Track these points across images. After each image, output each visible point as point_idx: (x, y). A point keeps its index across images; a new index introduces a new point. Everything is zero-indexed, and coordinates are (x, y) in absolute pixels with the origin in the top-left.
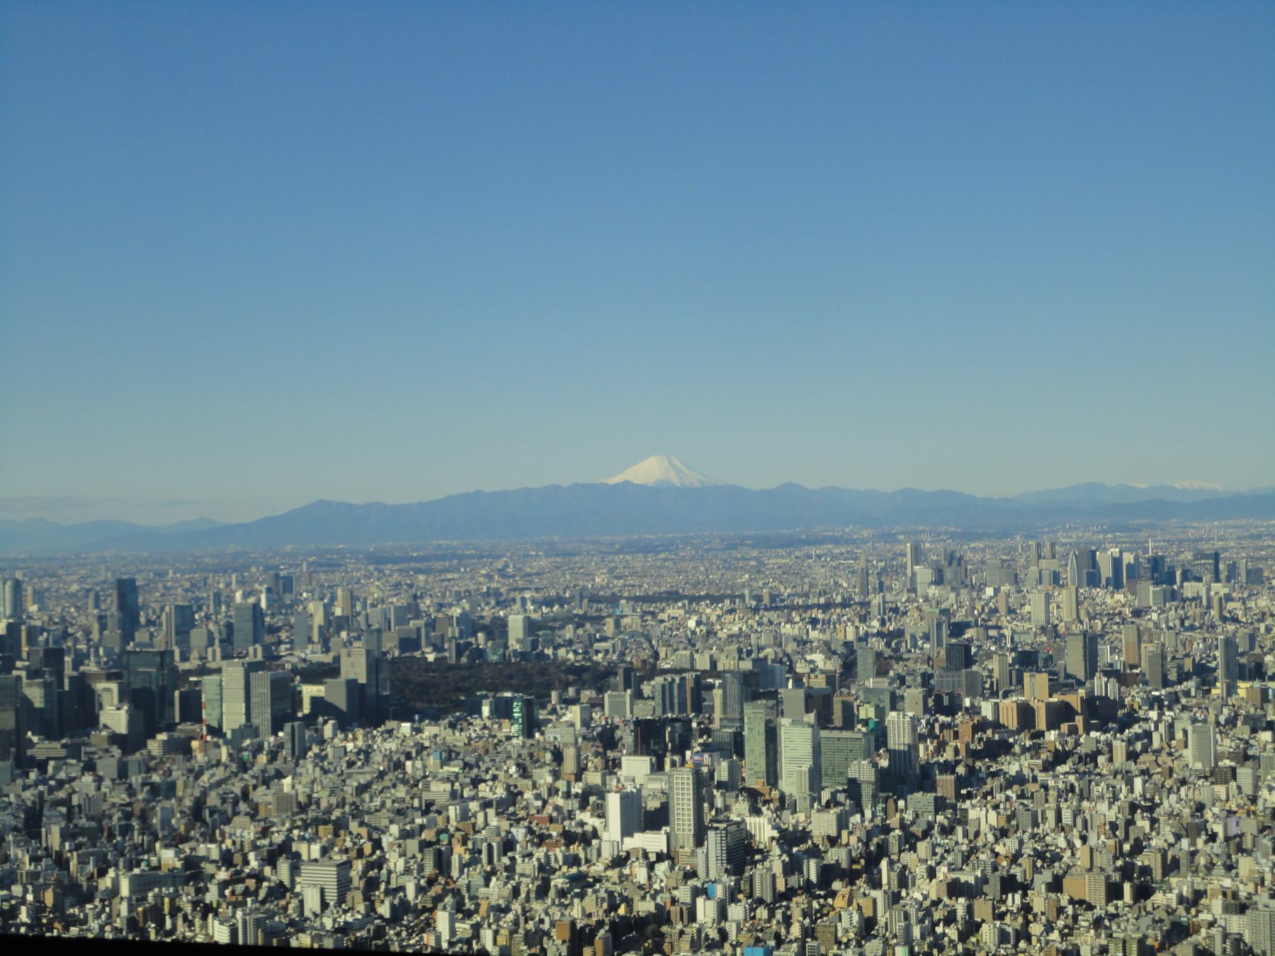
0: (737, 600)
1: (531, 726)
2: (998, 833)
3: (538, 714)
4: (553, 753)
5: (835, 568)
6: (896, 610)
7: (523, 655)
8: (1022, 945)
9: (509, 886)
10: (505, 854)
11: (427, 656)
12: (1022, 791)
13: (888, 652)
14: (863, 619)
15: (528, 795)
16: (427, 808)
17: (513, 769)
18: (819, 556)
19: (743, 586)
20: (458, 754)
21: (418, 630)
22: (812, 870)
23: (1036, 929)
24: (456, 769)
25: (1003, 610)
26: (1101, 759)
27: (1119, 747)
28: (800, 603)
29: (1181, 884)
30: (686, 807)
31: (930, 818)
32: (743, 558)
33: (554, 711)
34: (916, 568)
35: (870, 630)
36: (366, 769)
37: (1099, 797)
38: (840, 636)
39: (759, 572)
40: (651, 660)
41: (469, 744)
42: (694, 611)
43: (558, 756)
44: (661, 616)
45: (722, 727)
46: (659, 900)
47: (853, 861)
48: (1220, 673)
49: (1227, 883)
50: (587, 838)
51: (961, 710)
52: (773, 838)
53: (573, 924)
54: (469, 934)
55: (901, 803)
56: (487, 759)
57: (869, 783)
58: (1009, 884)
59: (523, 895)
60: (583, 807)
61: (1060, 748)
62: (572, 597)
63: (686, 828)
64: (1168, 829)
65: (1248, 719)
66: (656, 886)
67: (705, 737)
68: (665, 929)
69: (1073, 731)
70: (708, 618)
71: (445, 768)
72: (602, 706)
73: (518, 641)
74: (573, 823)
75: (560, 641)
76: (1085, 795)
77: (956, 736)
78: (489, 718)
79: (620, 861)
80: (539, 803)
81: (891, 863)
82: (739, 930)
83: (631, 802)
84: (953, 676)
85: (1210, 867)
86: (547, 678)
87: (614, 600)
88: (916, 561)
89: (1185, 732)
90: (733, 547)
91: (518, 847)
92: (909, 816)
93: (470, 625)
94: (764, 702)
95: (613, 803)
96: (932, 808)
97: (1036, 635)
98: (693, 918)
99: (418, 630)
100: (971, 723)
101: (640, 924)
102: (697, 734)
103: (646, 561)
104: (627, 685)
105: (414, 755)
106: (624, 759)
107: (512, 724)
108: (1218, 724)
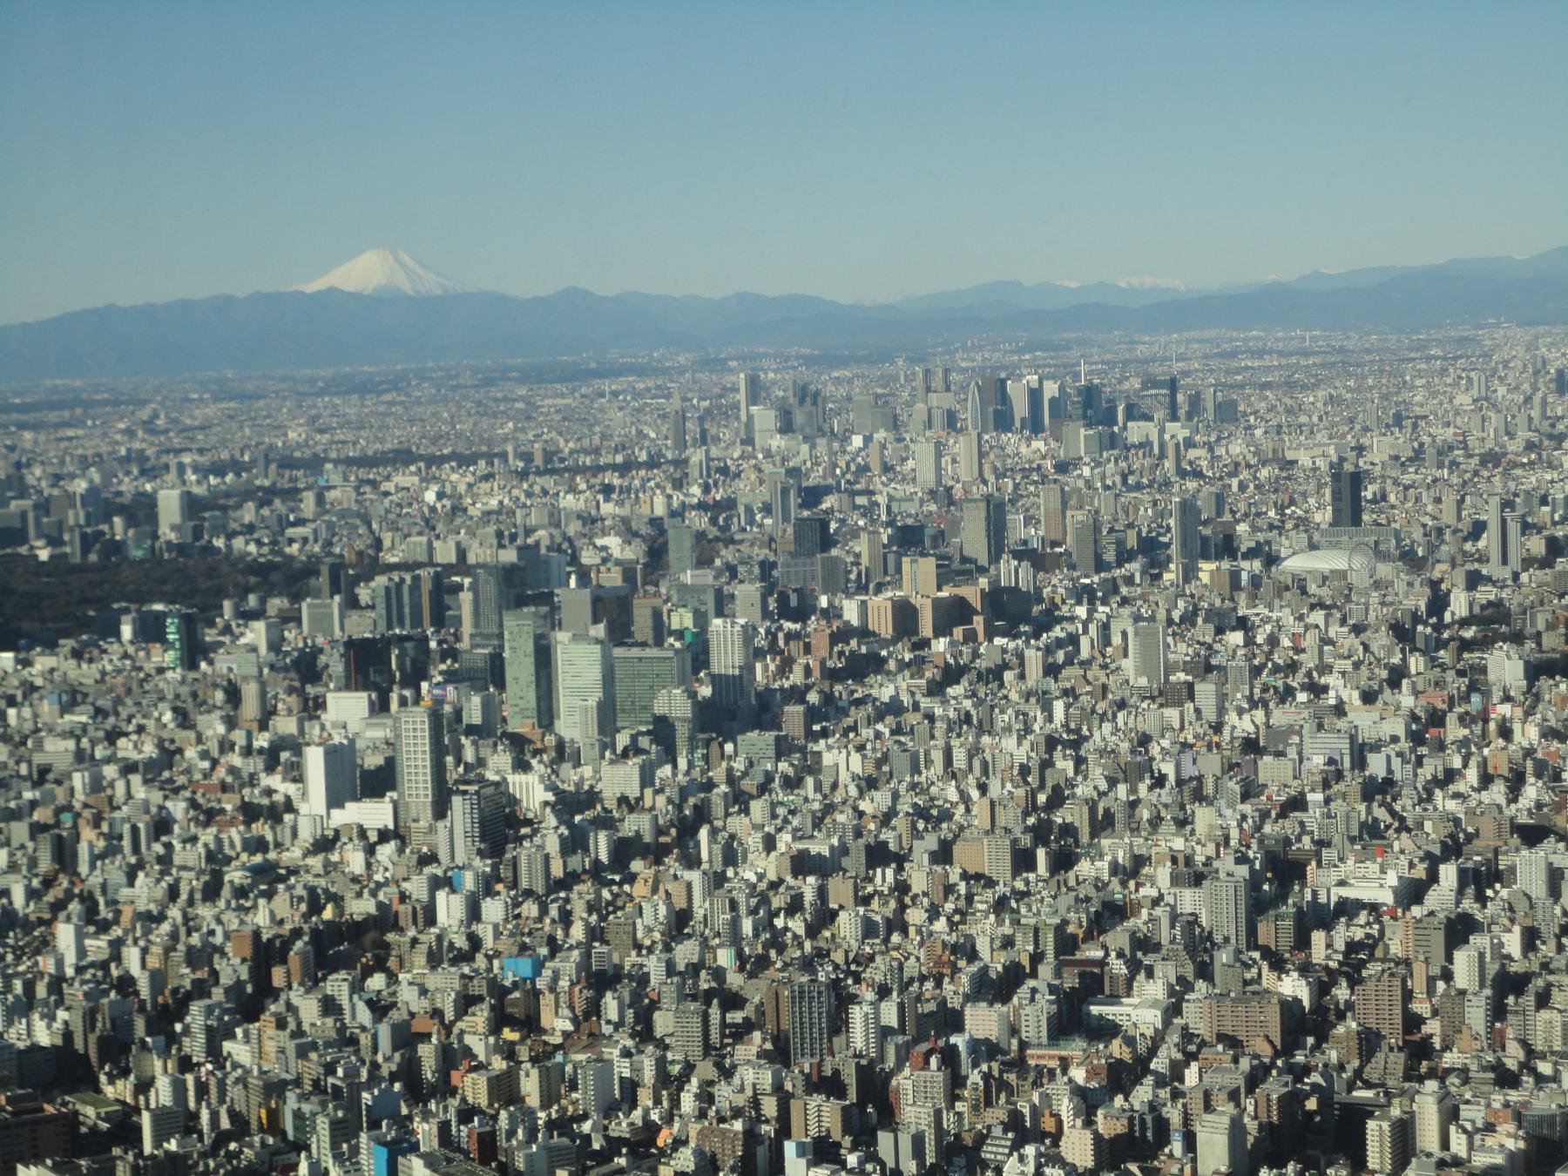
0: (496, 461)
1: (194, 652)
2: (863, 784)
3: (204, 635)
4: (226, 691)
5: (639, 410)
6: (724, 471)
7: (181, 549)
8: (896, 938)
9: (164, 884)
10: (157, 839)
11: (38, 552)
12: (899, 724)
13: (713, 532)
14: (678, 484)
15: (191, 753)
16: (42, 776)
17: (168, 717)
18: (615, 394)
19: (505, 439)
20: (86, 695)
21: (24, 515)
22: (602, 845)
23: (915, 916)
24: (84, 719)
25: (876, 468)
26: (1008, 676)
27: (1034, 658)
28: (588, 462)
29: (1116, 848)
30: (420, 763)
31: (769, 767)
32: (506, 399)
33: (227, 630)
34: (754, 409)
35: (687, 501)
37: (1003, 729)
38: (645, 510)
39: (529, 418)
40: (370, 552)
41: (101, 681)
42: (434, 478)
43: (234, 695)
44: (388, 486)
45: (474, 646)
46: (381, 897)
47: (660, 831)
48: (1174, 550)
49: (1179, 844)
50: (276, 812)
51: (814, 612)
52: (546, 803)
53: (257, 934)
54: (105, 955)
55: (729, 748)
56: (129, 701)
57: (683, 720)
58: (878, 855)
59: (184, 896)
60: (270, 768)
61: (952, 661)
62: (253, 462)
63: (422, 792)
64: (1099, 771)
65: (1211, 615)
66: (378, 877)
67: (449, 662)
68: (391, 937)
69: (970, 637)
70: (454, 488)
71: (67, 717)
72: (299, 621)
73: (174, 528)
74: (256, 792)
75: (234, 526)
76: (986, 727)
77: (808, 649)
78: (132, 642)
79: (325, 844)
80: (206, 764)
81: (714, 832)
82: (497, 934)
83: (340, 758)
84: (804, 565)
85: (1156, 821)
87: (315, 464)
88: (753, 399)
89: (1124, 634)
90: (489, 382)
91: (176, 829)
92: (739, 765)
93: (101, 505)
94: (533, 609)
95: (314, 760)
96: (771, 753)
97: (922, 502)
98: (431, 920)
99: (24, 515)
100: (828, 631)
101: (356, 931)
102: (438, 657)
103: (363, 405)
104: (335, 588)
105: (19, 698)
106: (330, 697)
108: (1170, 622)
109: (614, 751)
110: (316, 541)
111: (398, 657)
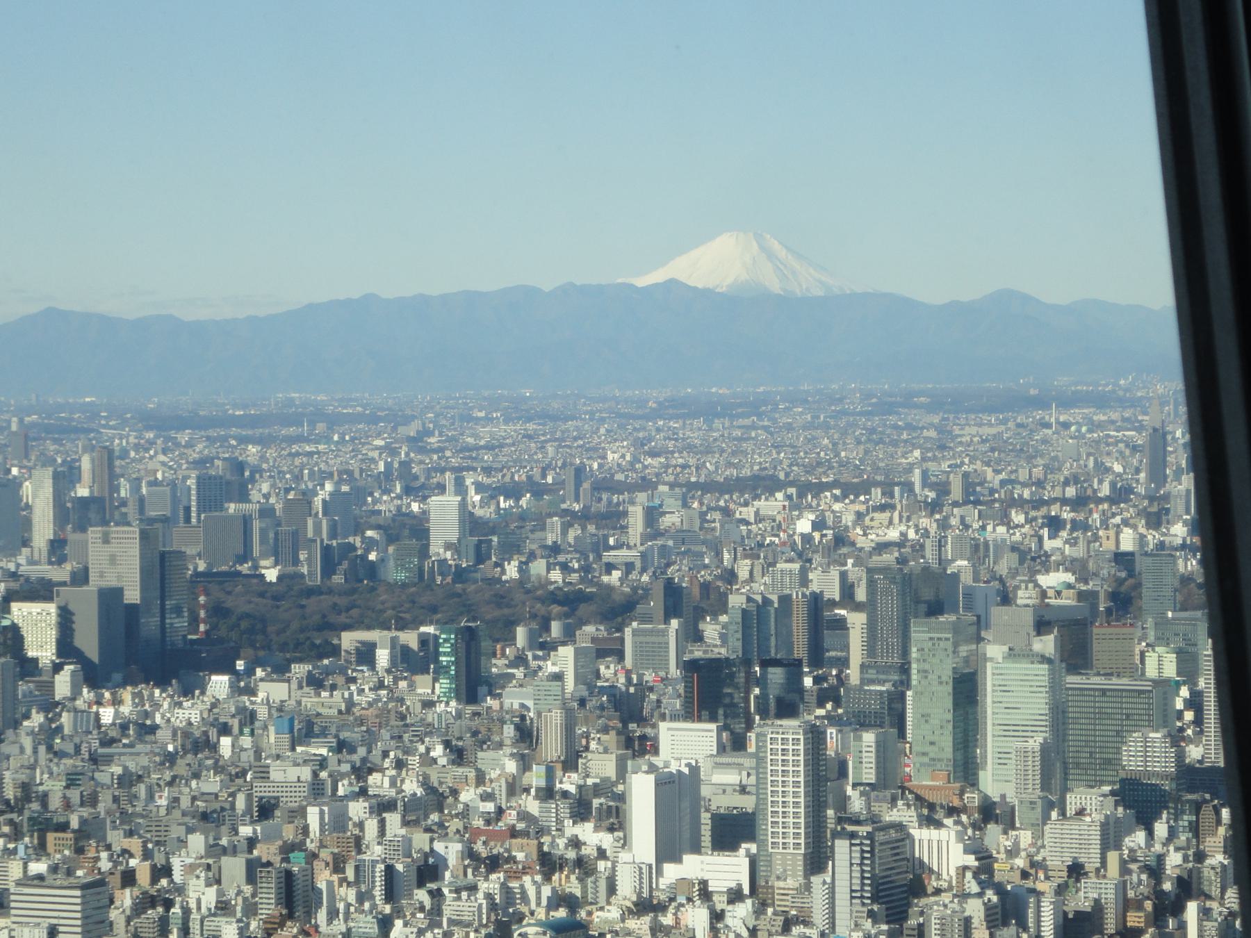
4: (518, 728)
15: (468, 795)
16: (265, 810)
17: (438, 751)
24: (324, 751)
36: (139, 747)
43: (526, 734)
45: (864, 681)
56: (385, 734)
57: (1165, 776)
67: (829, 706)
71: (299, 749)
72: (620, 655)
74: (561, 842)
86: (506, 611)
104: (671, 610)
107: (435, 680)
109: (1063, 813)
110: (644, 570)
111: (756, 697)
